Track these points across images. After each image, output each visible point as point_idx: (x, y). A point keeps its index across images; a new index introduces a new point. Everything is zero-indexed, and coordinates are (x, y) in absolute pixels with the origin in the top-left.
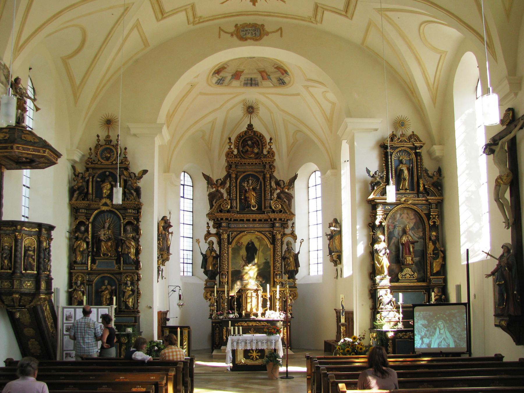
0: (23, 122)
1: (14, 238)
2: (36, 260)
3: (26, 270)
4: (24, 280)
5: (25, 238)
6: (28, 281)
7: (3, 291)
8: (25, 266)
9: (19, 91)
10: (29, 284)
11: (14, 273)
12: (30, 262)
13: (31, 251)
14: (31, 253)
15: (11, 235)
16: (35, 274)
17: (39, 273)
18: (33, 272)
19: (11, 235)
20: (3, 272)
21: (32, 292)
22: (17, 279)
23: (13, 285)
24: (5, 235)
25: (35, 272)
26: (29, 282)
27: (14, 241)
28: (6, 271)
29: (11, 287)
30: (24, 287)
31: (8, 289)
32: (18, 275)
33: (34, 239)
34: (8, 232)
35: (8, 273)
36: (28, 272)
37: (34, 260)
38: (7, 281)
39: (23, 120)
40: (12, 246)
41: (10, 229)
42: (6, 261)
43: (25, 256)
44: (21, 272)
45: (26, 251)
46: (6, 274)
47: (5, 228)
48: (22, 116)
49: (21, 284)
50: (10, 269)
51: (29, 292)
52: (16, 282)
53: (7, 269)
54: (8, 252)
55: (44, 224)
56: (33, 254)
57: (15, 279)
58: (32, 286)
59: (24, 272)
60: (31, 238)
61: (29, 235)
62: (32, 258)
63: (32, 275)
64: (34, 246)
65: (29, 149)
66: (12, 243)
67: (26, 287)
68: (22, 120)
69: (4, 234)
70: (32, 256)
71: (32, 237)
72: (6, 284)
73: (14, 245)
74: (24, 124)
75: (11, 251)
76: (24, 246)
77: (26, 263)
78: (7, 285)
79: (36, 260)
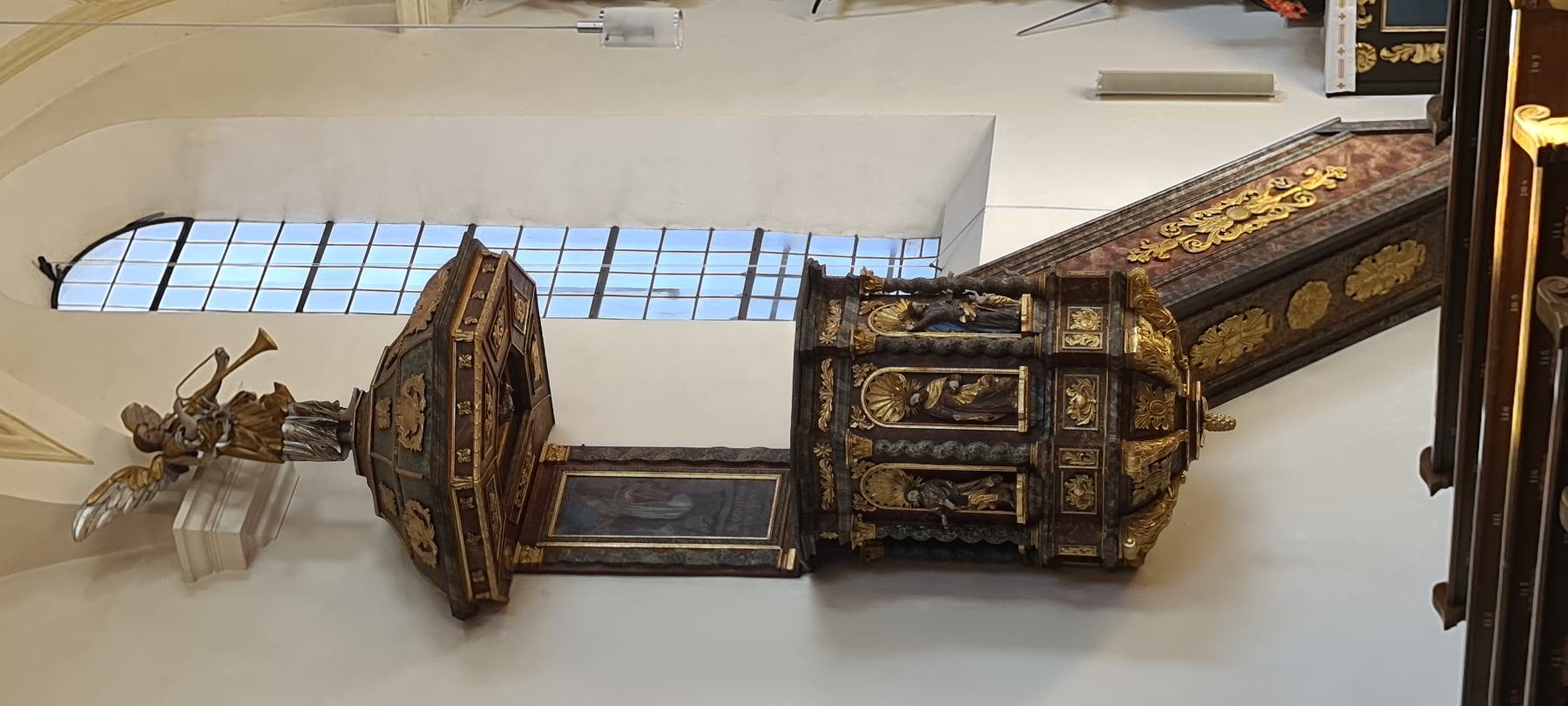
0: (335, 407)
1: (869, 464)
2: (966, 370)
3: (1012, 417)
4: (1059, 421)
5: (868, 421)
6: (1064, 401)
7: (1112, 504)
8: (997, 417)
9: (197, 437)
10: (1080, 398)
11: (1028, 468)
12: (977, 399)
13: (925, 397)
14: (935, 389)
15: (855, 477)
16: (1031, 373)
17: (1028, 357)
18: (1021, 386)
19: (855, 477)
20: (1027, 503)
21: (1115, 386)
22: (1056, 457)
23: (1080, 472)
24: (856, 496)
25: (1022, 371)
26: (1069, 398)
27: (882, 466)
28: (1019, 496)
29: (1091, 476)
30: (1091, 423)
31: (1100, 485)
32: (1034, 449)
33: (867, 377)
34: (843, 487)
35: (1026, 490)
36: (1021, 410)
37: (966, 379)
38: (1066, 489)
39: (327, 411)
40: (907, 471)
41: (829, 477)
42: (974, 498)
43: (952, 421)
44: (1027, 437)
45: (919, 413)
46: (1031, 496)
47: (828, 496)
48: (309, 414)
49: (1074, 439)
50: (1011, 478)
51: (1115, 401)
52: (1067, 462)
53: (1012, 493)
54: (931, 492)
55: (798, 341)
56: (939, 383)
57: (1056, 466)
58: (1087, 383)
59: (1022, 427)
60: (868, 390)
61: (850, 398)
62: (958, 391)
63: (1037, 386)
64: (902, 377)
65: (462, 417)
66: (891, 469)
67: (1090, 410)
68: (325, 415)
69: (853, 498)
70: (946, 387)
71: (861, 387)
72: (1078, 492)
73: (902, 465)
74: (345, 403)
75: (928, 476)
76: (902, 421)
77: (984, 418)
78: (1082, 488)
79: (966, 370)
